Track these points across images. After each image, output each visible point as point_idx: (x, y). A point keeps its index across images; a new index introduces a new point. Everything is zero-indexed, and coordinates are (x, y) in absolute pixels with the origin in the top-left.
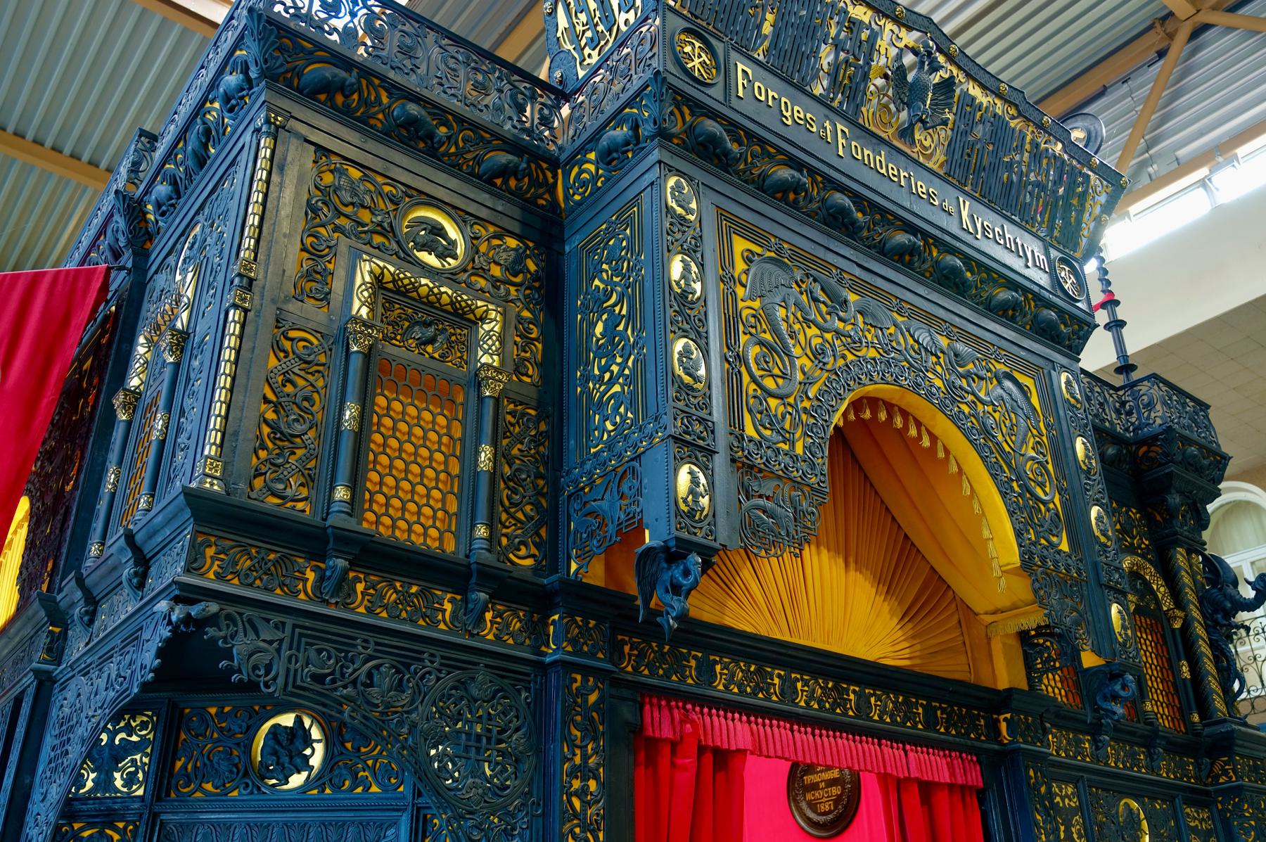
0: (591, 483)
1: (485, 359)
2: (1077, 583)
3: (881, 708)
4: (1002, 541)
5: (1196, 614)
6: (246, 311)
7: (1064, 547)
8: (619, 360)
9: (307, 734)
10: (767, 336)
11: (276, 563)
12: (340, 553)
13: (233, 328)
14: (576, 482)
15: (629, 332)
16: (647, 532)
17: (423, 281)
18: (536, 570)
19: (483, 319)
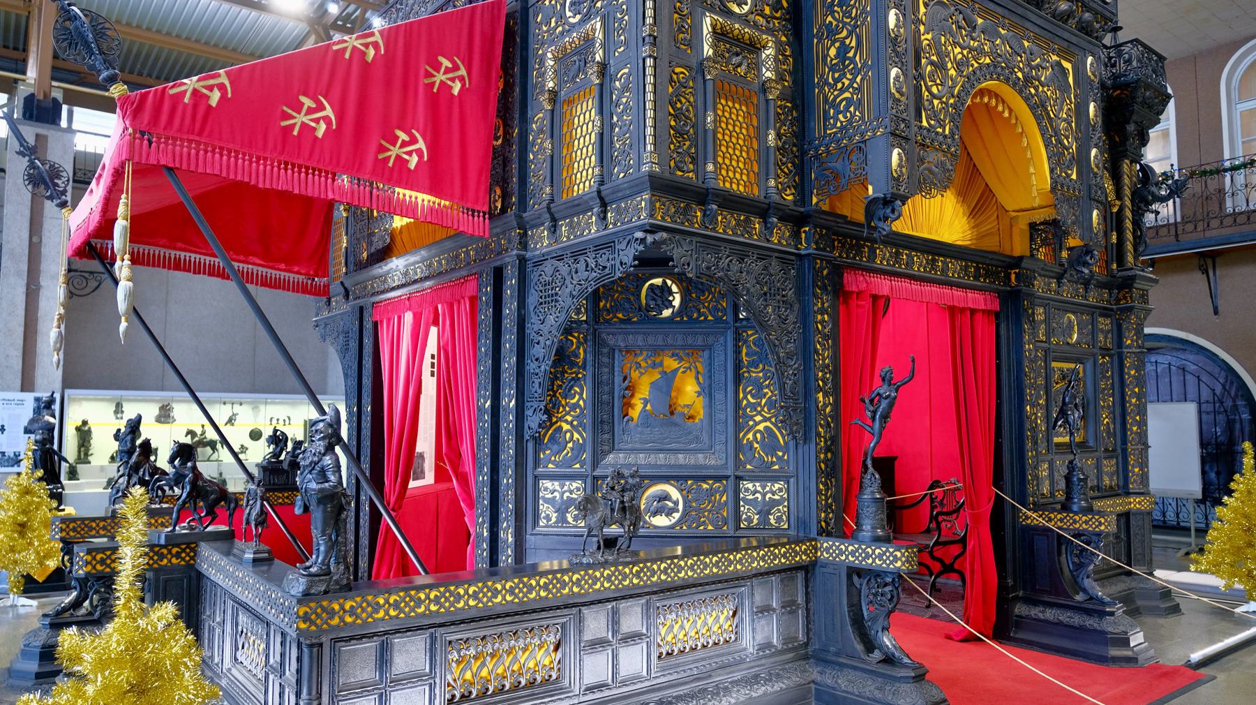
0: (828, 152)
1: (768, 74)
2: (1077, 199)
3: (954, 268)
4: (1041, 173)
5: (1128, 203)
6: (655, 59)
7: (1074, 177)
8: (849, 76)
9: (669, 289)
10: (934, 58)
11: (685, 209)
12: (714, 202)
13: (649, 71)
14: (817, 149)
15: (857, 58)
16: (870, 188)
17: (737, 26)
18: (795, 202)
19: (764, 47)
